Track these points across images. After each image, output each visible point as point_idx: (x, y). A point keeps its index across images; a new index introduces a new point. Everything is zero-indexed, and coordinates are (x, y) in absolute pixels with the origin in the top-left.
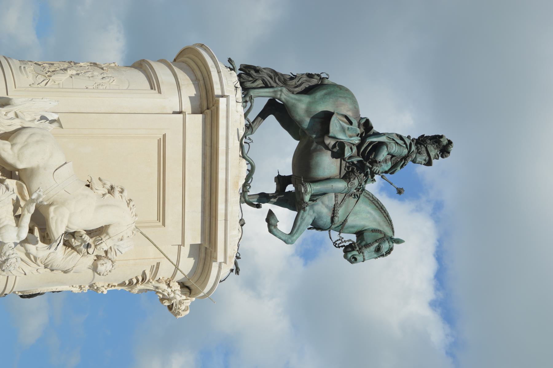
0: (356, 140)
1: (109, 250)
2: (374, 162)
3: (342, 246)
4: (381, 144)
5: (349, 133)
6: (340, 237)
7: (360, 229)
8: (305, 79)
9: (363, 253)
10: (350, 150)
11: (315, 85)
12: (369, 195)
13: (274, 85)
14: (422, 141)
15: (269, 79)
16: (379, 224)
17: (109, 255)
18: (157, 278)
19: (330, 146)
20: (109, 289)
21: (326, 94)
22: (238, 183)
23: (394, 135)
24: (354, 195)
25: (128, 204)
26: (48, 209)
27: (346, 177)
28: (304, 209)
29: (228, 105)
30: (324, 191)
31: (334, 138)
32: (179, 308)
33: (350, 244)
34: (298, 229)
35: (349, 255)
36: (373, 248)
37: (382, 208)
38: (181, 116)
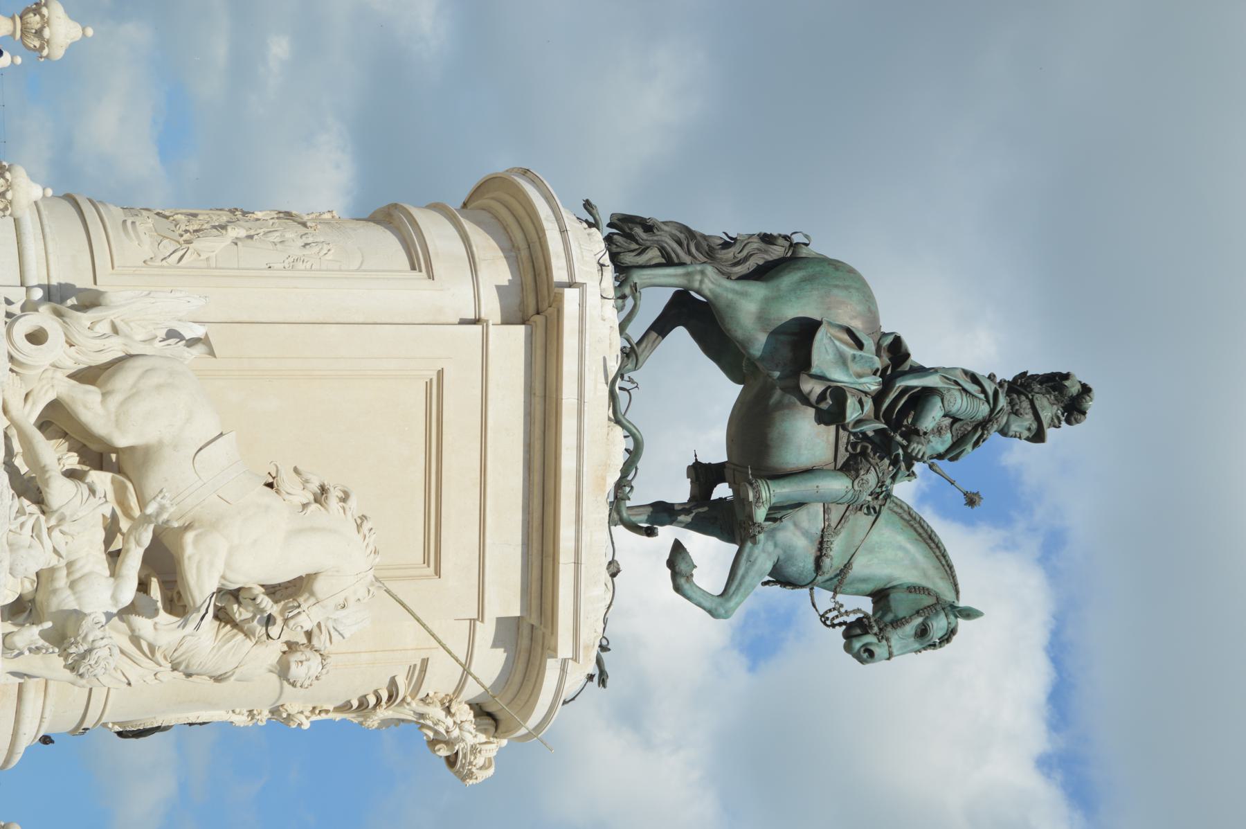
1: (316, 631)
2: (913, 433)
3: (840, 624)
4: (926, 394)
5: (855, 368)
6: (836, 603)
7: (880, 585)
8: (755, 246)
9: (887, 640)
10: (858, 406)
11: (778, 261)
12: (901, 507)
13: (687, 259)
14: (1021, 386)
15: (675, 246)
17: (315, 641)
18: (422, 695)
19: (813, 398)
20: (315, 718)
22: (604, 479)
23: (959, 373)
24: (868, 508)
25: (359, 527)
26: (181, 538)
27: (850, 467)
29: (582, 305)
30: (799, 499)
31: (821, 378)
32: (470, 763)
33: (859, 620)
34: (740, 584)
35: (857, 645)
36: (910, 628)
37: (930, 537)
38: (478, 329)
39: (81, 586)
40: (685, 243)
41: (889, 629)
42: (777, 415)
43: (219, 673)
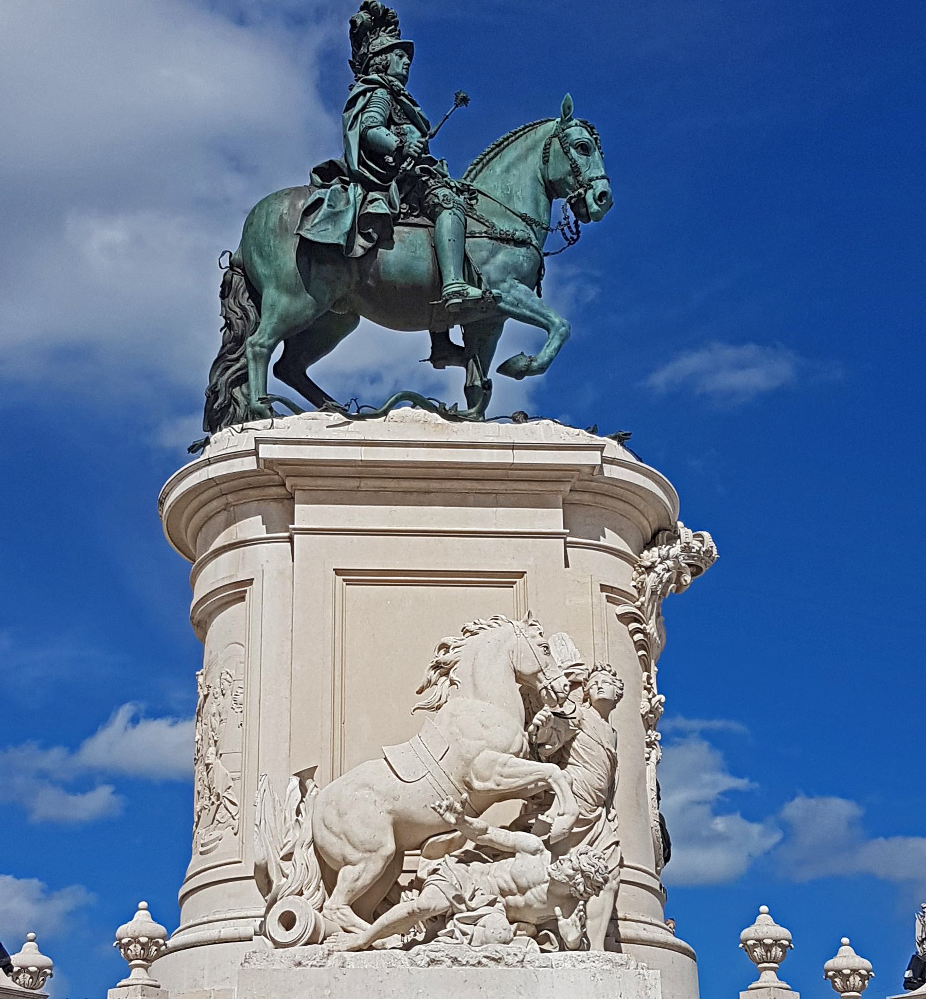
0: (355, 192)
1: (572, 678)
2: (400, 153)
3: (577, 226)
4: (364, 141)
5: (341, 206)
7: (541, 189)
9: (591, 180)
10: (376, 203)
16: (532, 149)
17: (581, 678)
18: (635, 592)
19: (370, 245)
20: (655, 691)
21: (261, 255)
23: (346, 115)
24: (471, 199)
25: (474, 634)
26: (479, 791)
28: (497, 299)
29: (275, 441)
30: (460, 258)
31: (350, 236)
32: (698, 552)
34: (538, 313)
36: (581, 160)
38: (296, 537)
39: (523, 882)
42: (383, 278)
43: (608, 762)
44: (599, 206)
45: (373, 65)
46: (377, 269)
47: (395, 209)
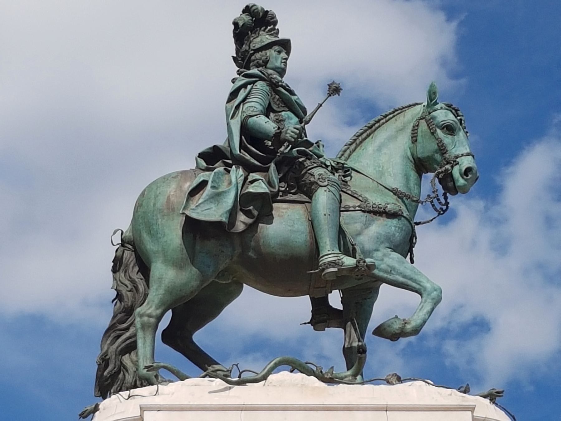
0: (237, 173)
2: (278, 138)
3: (446, 198)
4: (245, 129)
5: (223, 187)
7: (411, 166)
8: (122, 275)
9: (457, 157)
10: (256, 184)
12: (345, 151)
13: (132, 330)
14: (243, 60)
15: (120, 340)
16: (402, 129)
19: (250, 221)
21: (149, 233)
22: (314, 388)
23: (229, 105)
24: (344, 176)
27: (309, 191)
28: (371, 267)
31: (232, 214)
33: (440, 182)
34: (411, 279)
35: (461, 182)
36: (447, 140)
37: (370, 128)
40: (118, 332)
41: (447, 156)
44: (466, 180)
45: (254, 61)
46: (258, 242)
47: (274, 187)
